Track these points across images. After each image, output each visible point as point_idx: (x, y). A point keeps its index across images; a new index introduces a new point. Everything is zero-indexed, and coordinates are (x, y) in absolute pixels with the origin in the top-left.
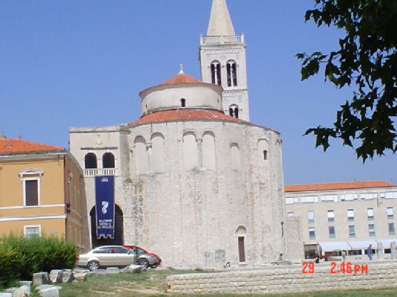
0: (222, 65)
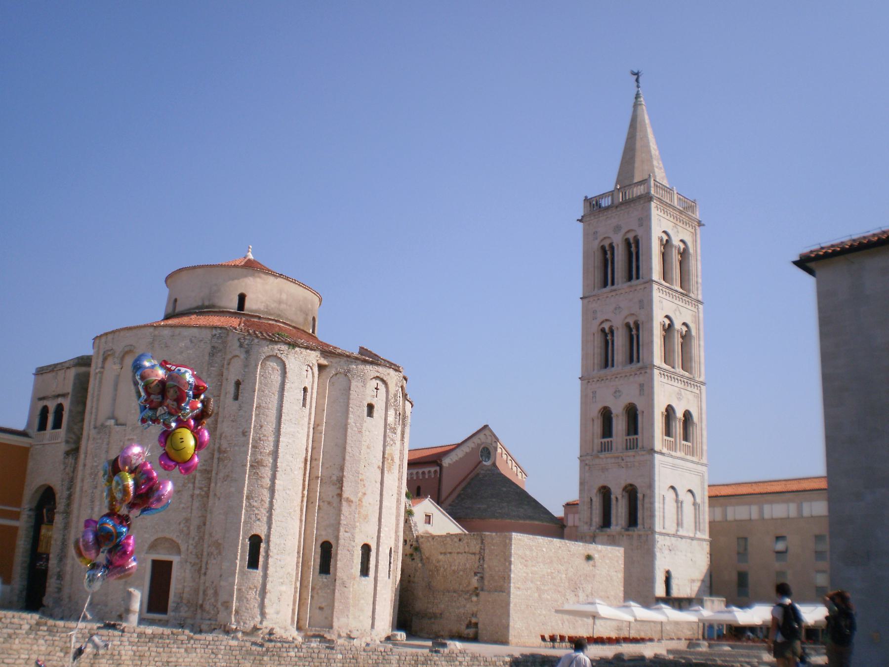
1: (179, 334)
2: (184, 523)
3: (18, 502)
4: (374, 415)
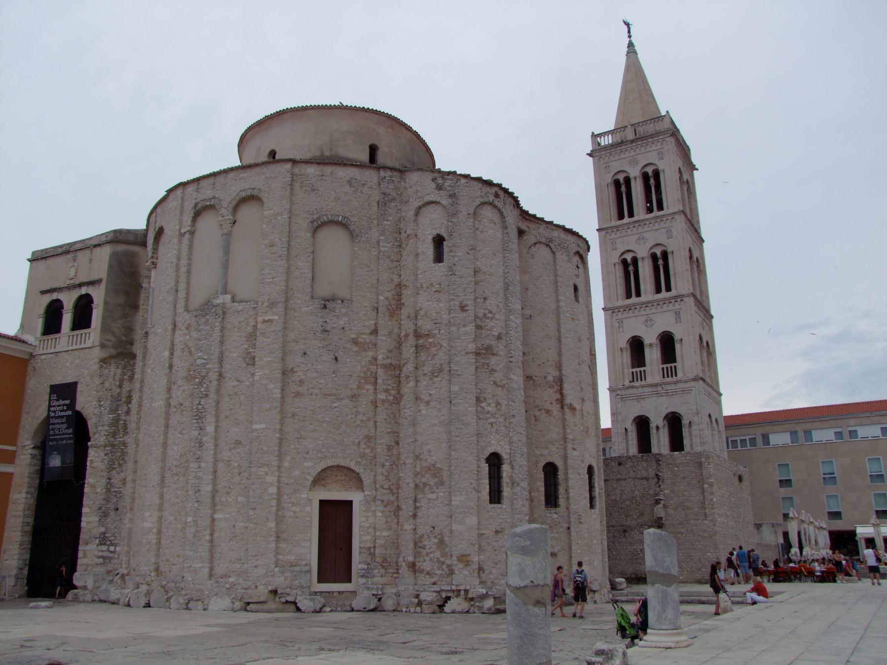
0: (632, 176)
1: (331, 174)
2: (365, 444)
3: (13, 439)
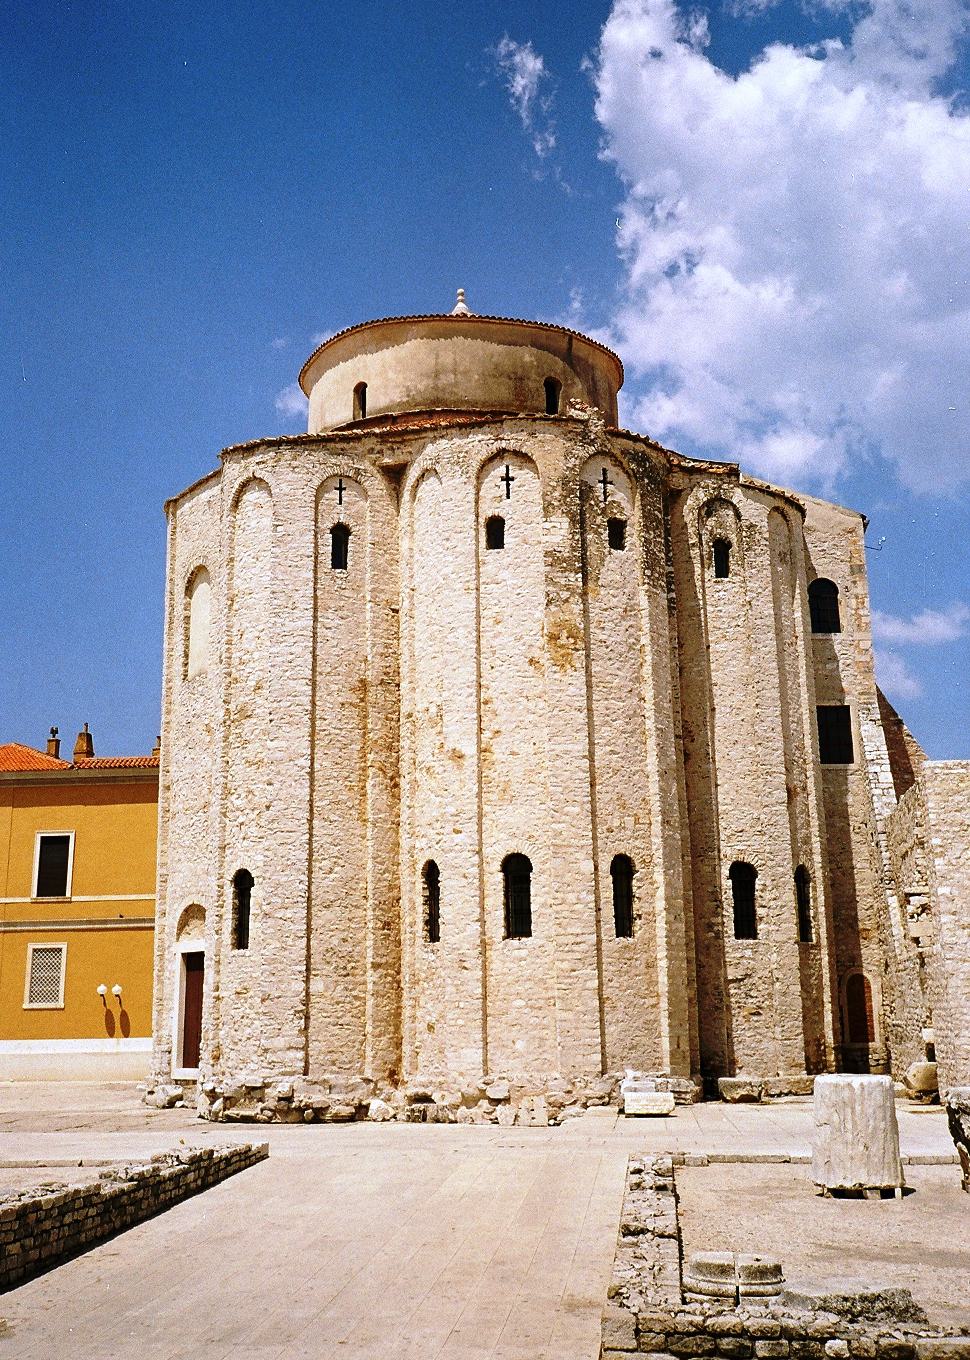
4: (508, 539)
